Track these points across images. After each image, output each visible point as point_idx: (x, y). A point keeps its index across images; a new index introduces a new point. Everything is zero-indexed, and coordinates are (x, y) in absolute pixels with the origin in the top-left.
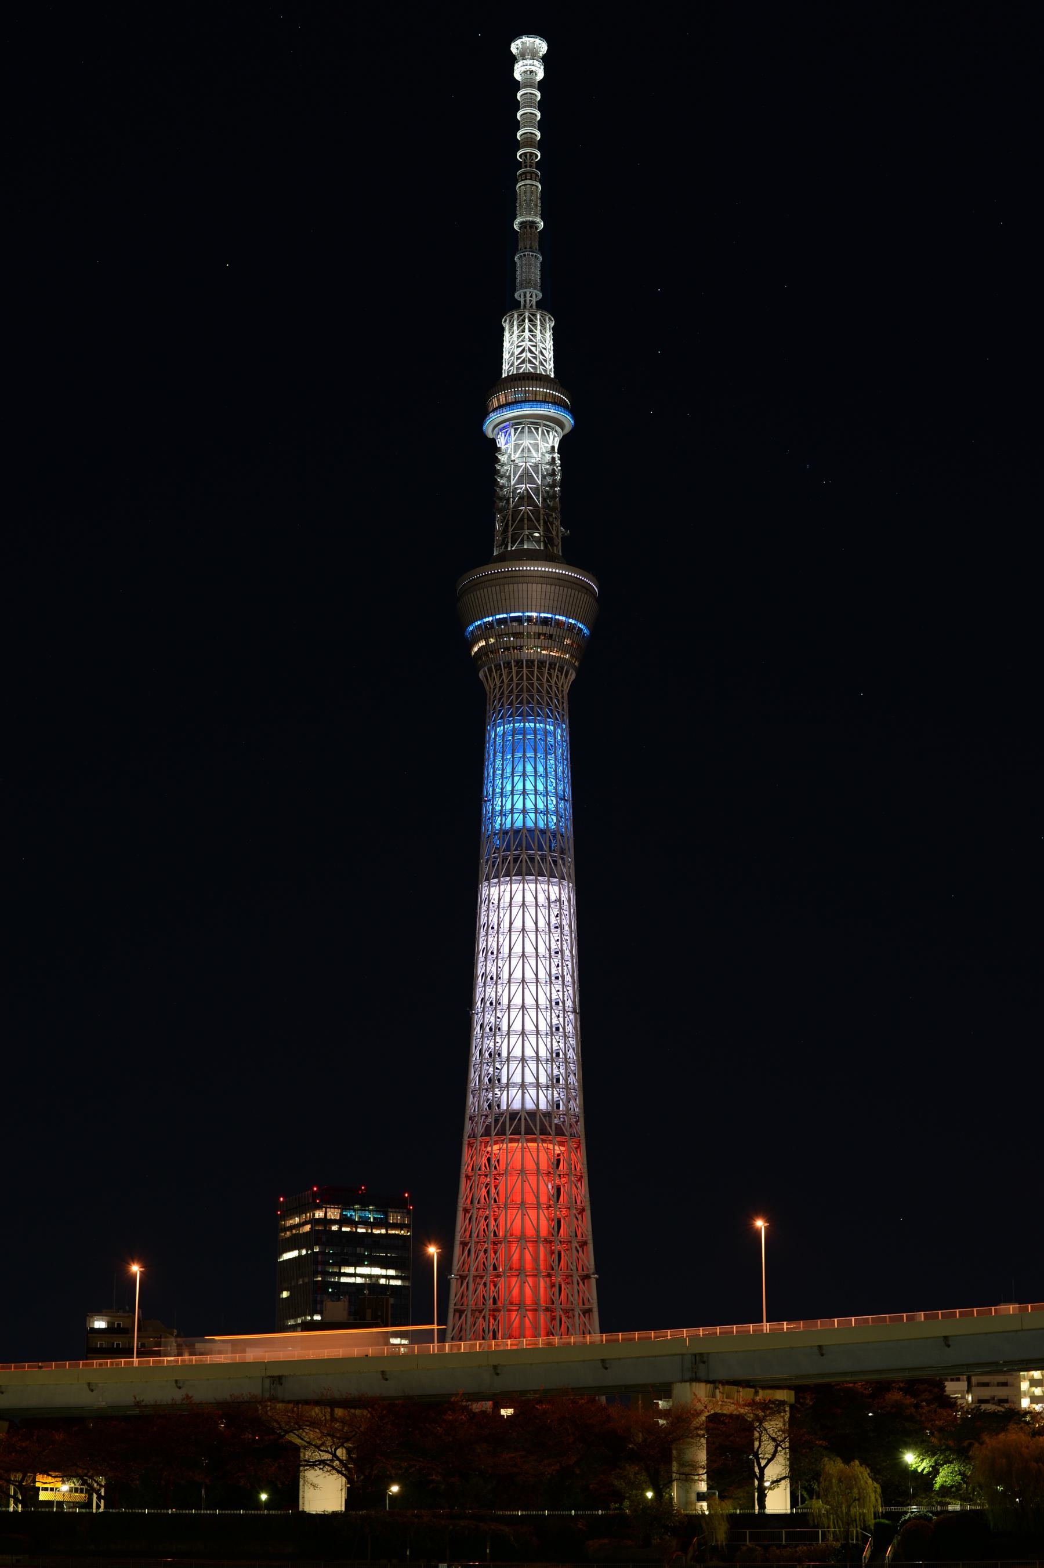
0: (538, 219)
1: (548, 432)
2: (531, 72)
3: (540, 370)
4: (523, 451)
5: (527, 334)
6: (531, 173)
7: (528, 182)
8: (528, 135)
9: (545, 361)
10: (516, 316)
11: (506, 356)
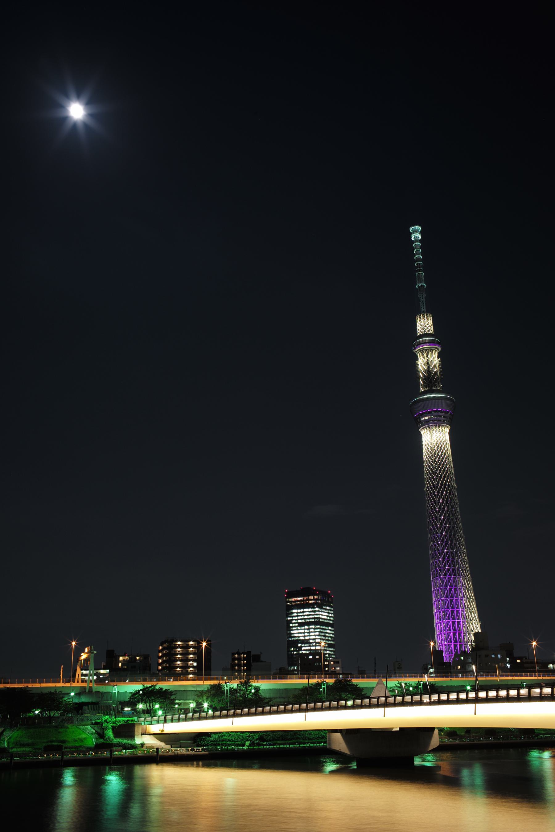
1: (435, 352)
2: (417, 237)
3: (430, 332)
4: (433, 358)
11: (418, 328)
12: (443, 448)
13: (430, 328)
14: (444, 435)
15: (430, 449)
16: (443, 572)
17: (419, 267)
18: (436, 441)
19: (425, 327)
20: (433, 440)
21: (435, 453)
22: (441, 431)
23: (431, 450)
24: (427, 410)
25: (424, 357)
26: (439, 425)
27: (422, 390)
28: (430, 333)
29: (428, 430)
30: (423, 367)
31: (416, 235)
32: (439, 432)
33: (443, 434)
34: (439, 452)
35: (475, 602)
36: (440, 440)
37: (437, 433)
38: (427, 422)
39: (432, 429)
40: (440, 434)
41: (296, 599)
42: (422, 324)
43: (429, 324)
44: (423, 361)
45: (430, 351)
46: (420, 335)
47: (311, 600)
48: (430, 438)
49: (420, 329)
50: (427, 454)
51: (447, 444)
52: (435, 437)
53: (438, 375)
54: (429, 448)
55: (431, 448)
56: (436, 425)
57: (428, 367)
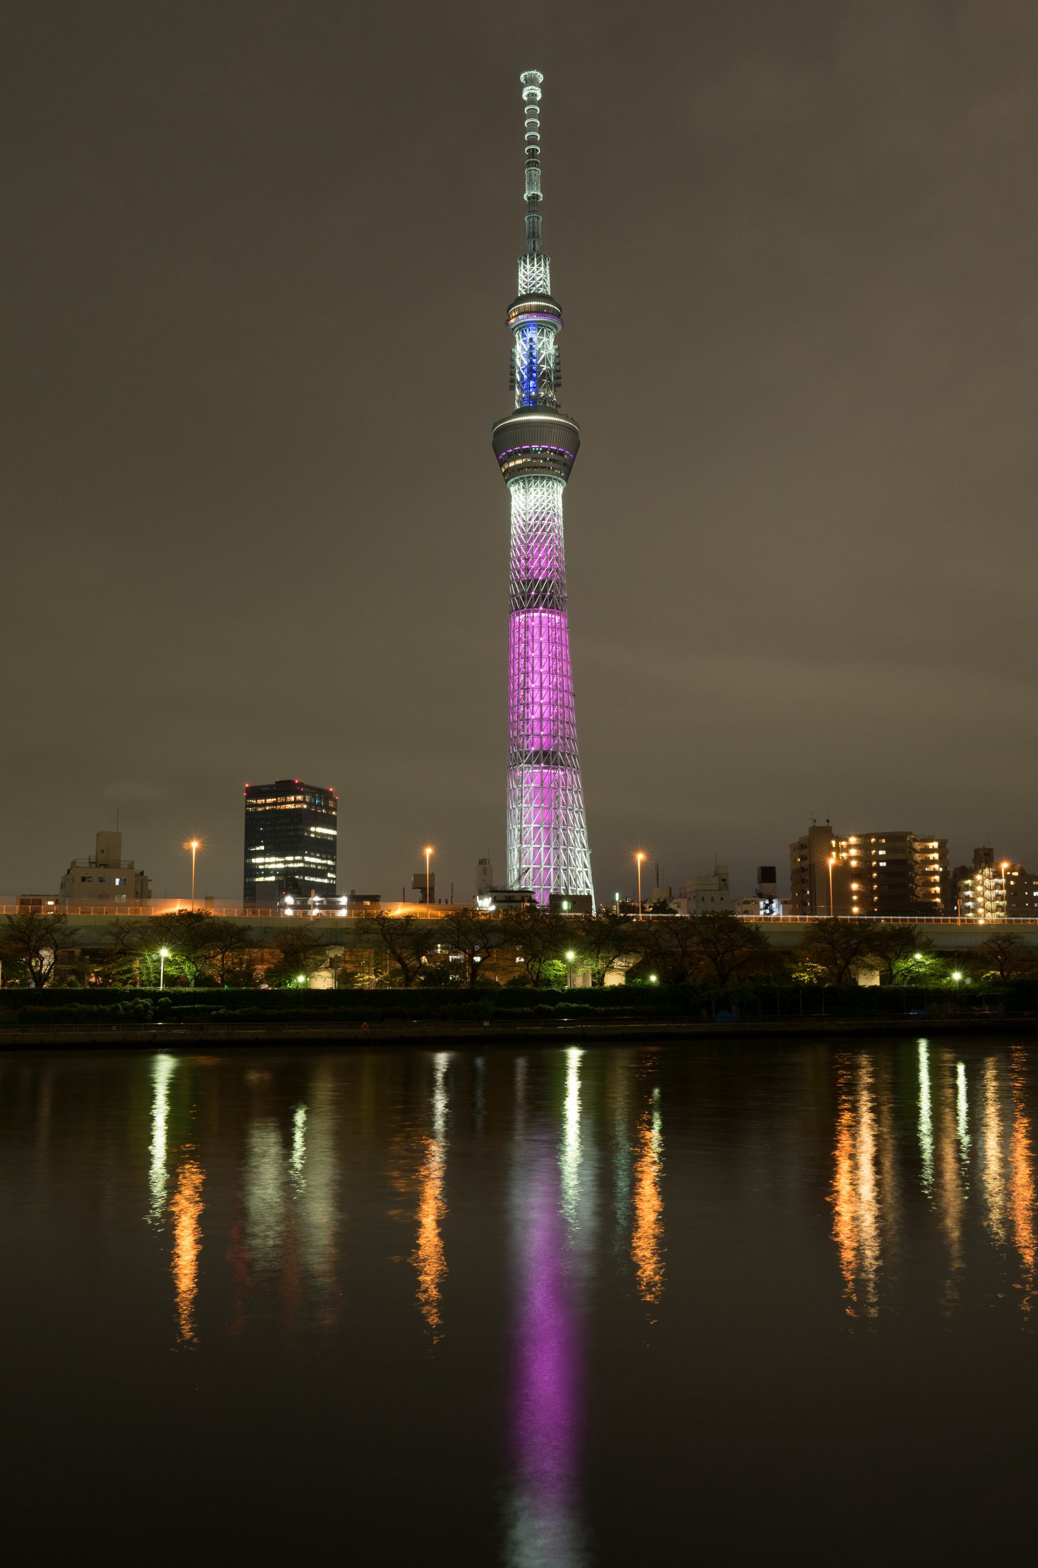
0: (540, 194)
2: (533, 94)
3: (542, 290)
6: (534, 162)
7: (532, 168)
8: (532, 137)
9: (547, 286)
10: (528, 257)
11: (520, 282)
12: (546, 522)
13: (542, 282)
14: (551, 497)
15: (522, 523)
16: (526, 757)
17: (531, 156)
18: (534, 508)
19: (533, 279)
20: (529, 505)
21: (530, 531)
22: (545, 489)
23: (525, 526)
24: (530, 446)
25: (525, 341)
26: (543, 478)
27: (518, 406)
28: (541, 293)
29: (521, 486)
30: (522, 361)
31: (531, 89)
32: (541, 490)
33: (549, 494)
34: (537, 530)
35: (584, 815)
36: (543, 507)
37: (537, 492)
38: (519, 469)
39: (528, 485)
40: (543, 494)
41: (263, 801)
42: (528, 273)
43: (542, 275)
44: (524, 350)
45: (539, 329)
46: (522, 296)
47: (291, 803)
48: (523, 503)
49: (523, 285)
50: (515, 534)
51: (555, 514)
52: (534, 501)
53: (550, 380)
54: (521, 521)
55: (524, 521)
56: (537, 477)
57: (531, 363)
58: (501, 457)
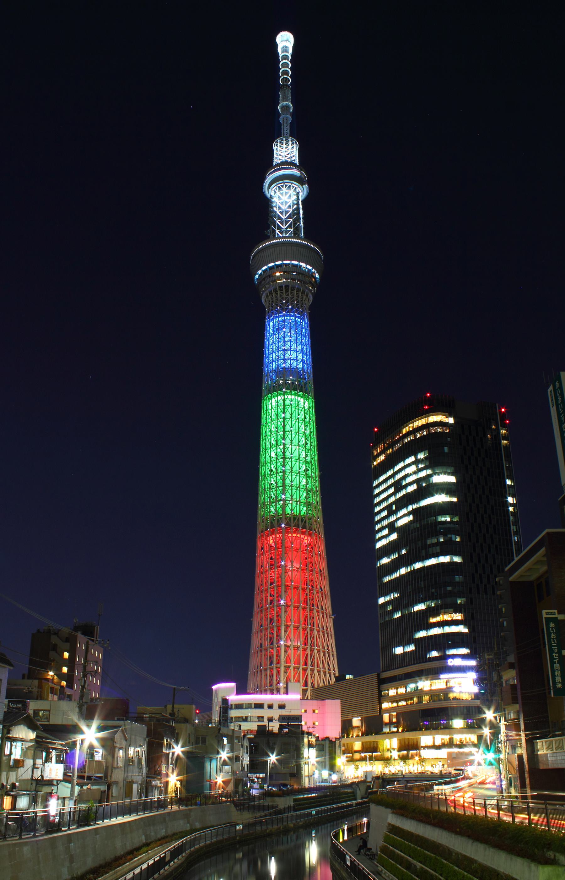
0: (291, 104)
2: (286, 47)
5: (290, 147)
10: (284, 139)
25: (282, 194)
43: (294, 154)
49: (280, 157)
58: (257, 276)
